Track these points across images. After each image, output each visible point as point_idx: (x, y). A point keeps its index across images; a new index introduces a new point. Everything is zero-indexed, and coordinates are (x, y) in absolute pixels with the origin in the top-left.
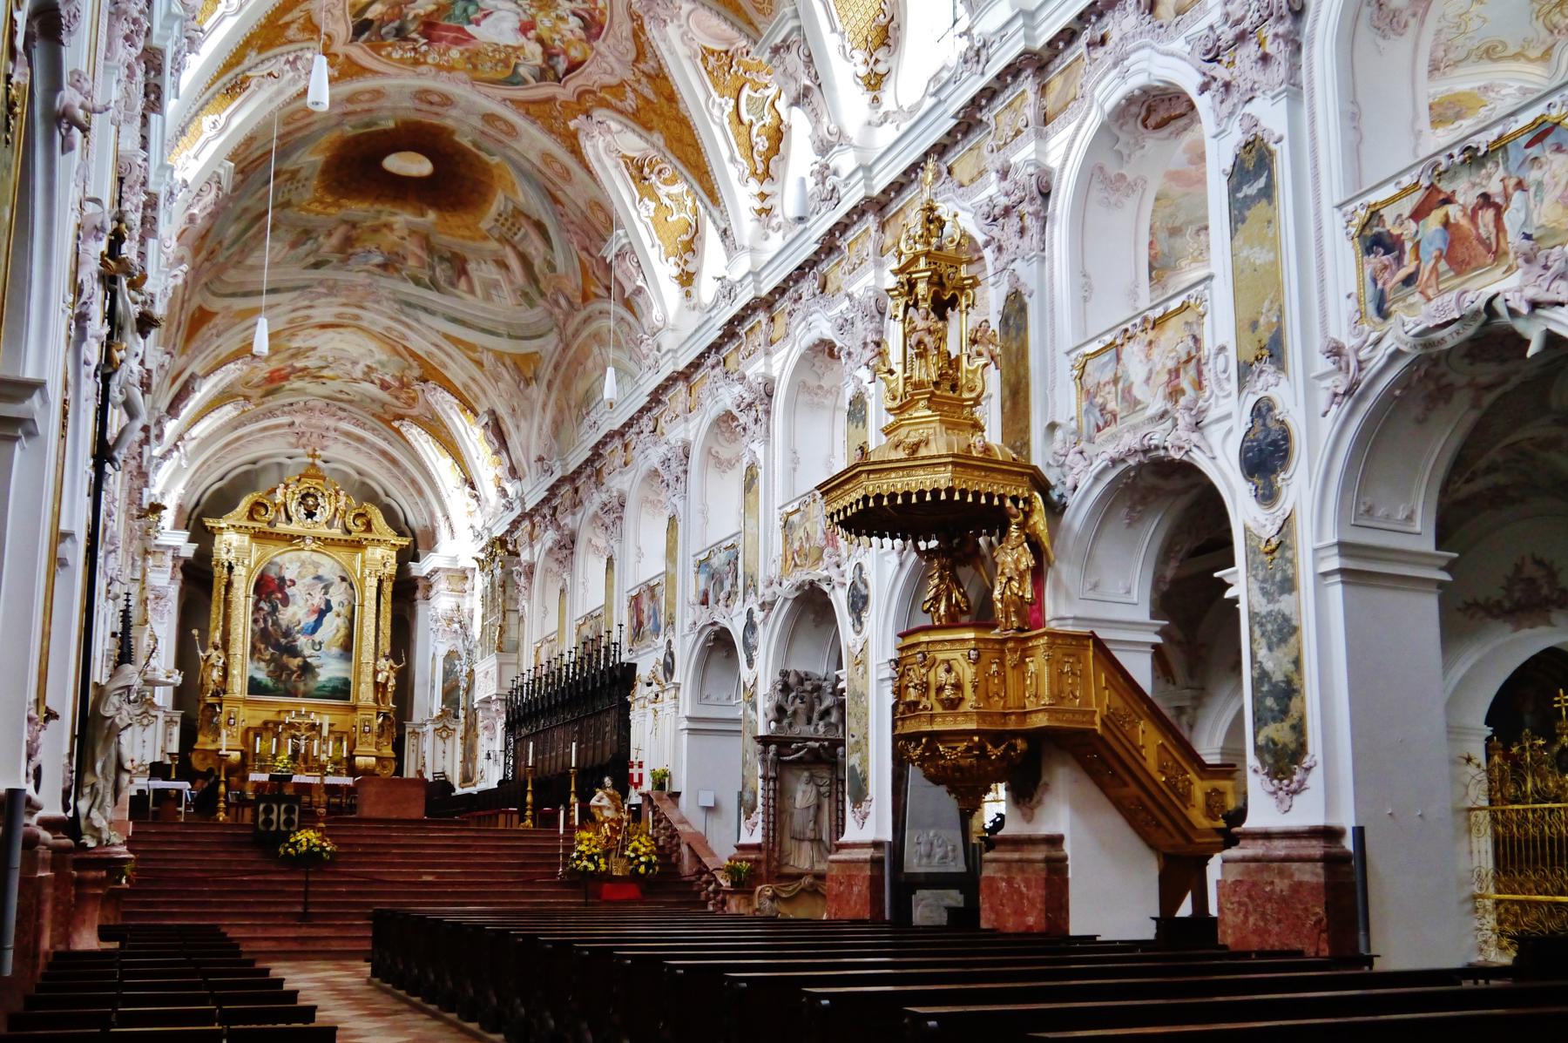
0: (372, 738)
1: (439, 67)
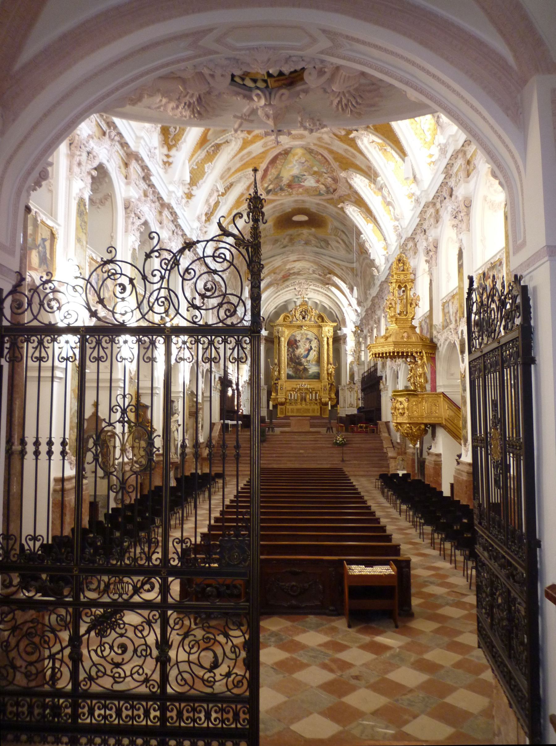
0: (328, 392)
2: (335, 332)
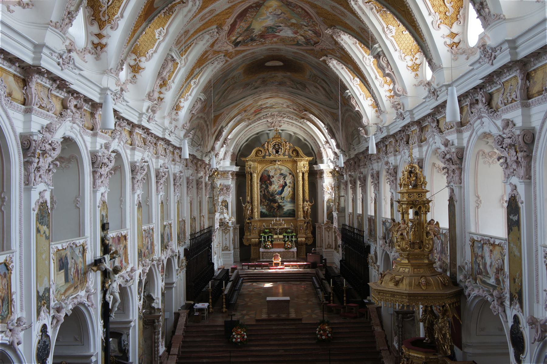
1: (271, 43)
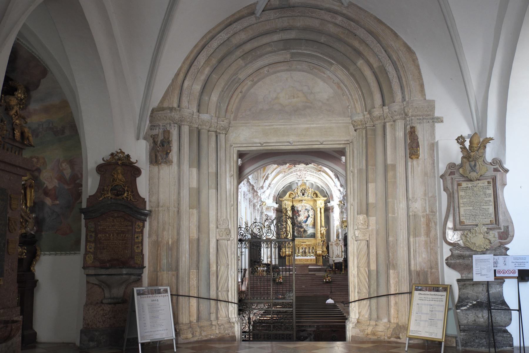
0: (320, 247)
2: (326, 203)
